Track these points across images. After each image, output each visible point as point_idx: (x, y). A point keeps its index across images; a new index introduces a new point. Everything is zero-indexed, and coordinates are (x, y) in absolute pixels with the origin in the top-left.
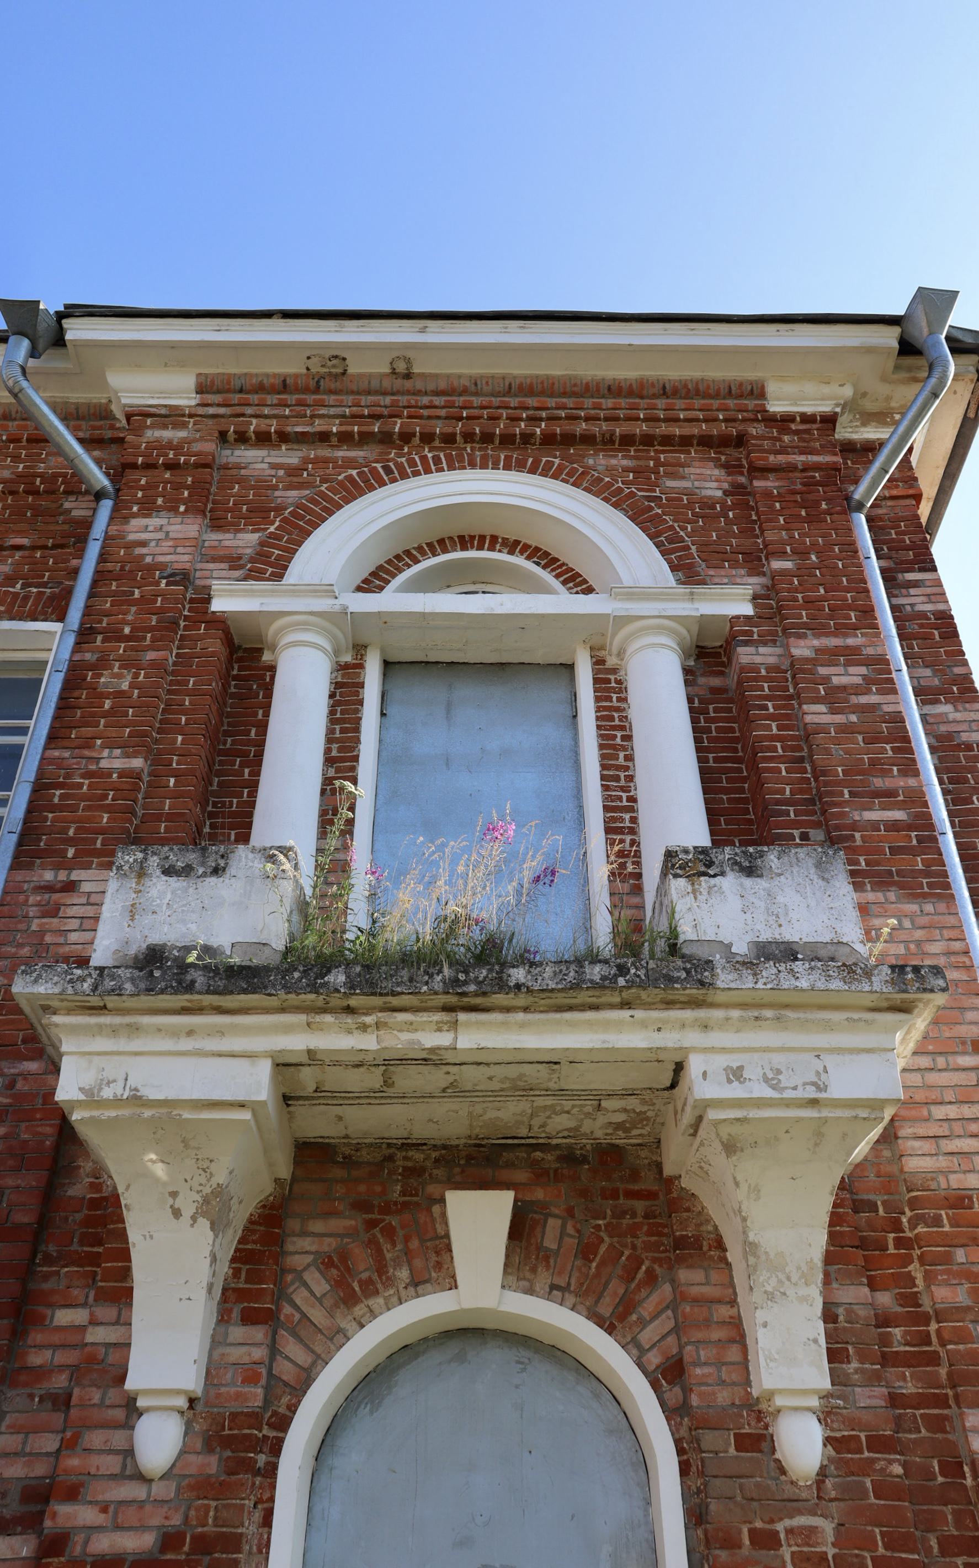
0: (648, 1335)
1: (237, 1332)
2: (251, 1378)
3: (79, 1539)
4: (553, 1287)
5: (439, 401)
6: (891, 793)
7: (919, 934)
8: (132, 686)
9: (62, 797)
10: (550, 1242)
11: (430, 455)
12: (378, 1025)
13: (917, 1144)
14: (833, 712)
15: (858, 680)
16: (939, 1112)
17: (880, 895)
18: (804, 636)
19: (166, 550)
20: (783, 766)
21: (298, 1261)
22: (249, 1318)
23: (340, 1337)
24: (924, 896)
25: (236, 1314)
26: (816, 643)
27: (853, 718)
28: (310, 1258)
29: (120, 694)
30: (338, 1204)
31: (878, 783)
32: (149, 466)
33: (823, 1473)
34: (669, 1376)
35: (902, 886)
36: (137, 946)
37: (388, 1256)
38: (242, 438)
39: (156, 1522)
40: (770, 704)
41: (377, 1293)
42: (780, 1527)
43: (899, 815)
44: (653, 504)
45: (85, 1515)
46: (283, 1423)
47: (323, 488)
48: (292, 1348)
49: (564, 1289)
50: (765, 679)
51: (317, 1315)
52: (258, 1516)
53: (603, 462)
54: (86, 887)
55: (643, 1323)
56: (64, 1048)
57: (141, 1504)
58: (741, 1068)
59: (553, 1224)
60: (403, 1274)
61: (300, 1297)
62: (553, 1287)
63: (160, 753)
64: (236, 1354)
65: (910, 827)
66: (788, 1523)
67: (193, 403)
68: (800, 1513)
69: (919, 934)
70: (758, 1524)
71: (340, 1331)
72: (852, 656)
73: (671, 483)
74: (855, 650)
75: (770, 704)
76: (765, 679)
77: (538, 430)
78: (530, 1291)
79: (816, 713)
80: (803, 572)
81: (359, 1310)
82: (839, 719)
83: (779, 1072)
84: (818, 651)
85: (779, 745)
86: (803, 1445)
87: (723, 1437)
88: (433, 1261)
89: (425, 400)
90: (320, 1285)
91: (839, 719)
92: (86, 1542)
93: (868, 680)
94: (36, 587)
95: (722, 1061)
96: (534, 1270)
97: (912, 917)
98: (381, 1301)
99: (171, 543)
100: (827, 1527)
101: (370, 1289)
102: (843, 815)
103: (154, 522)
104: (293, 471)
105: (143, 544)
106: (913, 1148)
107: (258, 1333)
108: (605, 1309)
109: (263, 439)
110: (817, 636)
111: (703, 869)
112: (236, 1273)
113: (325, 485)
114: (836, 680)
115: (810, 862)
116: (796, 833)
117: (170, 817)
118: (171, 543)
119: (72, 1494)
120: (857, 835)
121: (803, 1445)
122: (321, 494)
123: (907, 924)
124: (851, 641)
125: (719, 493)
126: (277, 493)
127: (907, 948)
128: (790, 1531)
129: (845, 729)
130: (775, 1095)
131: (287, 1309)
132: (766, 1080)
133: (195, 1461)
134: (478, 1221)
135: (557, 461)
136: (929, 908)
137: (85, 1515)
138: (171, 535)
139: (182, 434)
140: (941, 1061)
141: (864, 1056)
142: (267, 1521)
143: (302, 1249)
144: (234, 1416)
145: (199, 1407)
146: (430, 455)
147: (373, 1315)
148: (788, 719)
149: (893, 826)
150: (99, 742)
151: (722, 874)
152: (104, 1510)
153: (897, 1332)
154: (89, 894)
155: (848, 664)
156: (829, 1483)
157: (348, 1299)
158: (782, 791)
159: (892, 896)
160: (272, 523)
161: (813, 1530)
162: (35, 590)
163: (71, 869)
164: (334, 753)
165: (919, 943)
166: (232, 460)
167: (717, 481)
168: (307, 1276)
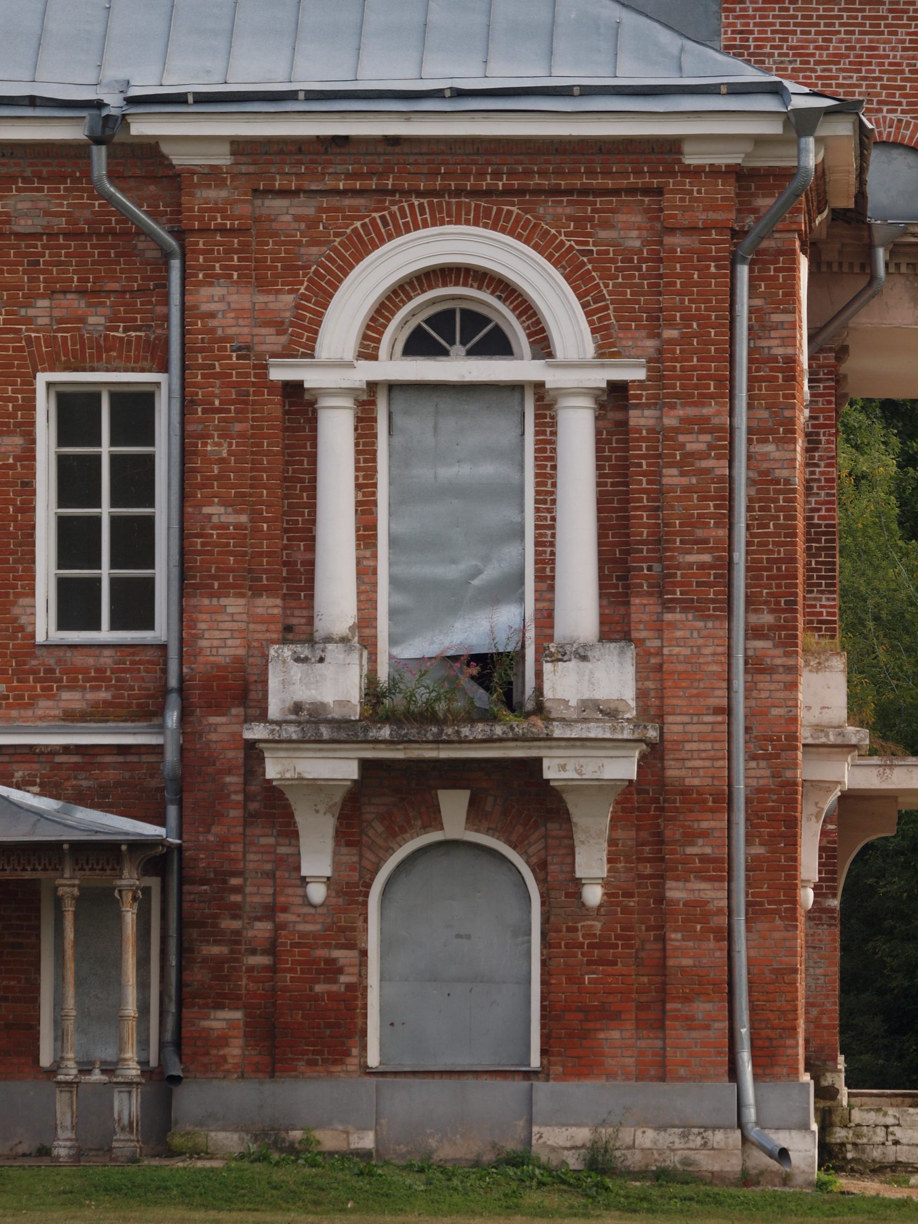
0: (532, 850)
1: (344, 850)
2: (353, 869)
3: (291, 925)
4: (489, 829)
5: (421, 159)
6: (706, 541)
7: (700, 642)
8: (230, 453)
9: (203, 544)
10: (488, 808)
11: (416, 203)
12: (405, 749)
13: (673, 763)
14: (683, 474)
15: (703, 447)
16: (688, 746)
17: (684, 615)
18: (673, 406)
19: (231, 322)
20: (645, 514)
21: (368, 817)
22: (349, 844)
23: (390, 851)
24: (709, 616)
25: (343, 842)
26: (681, 412)
27: (694, 481)
28: (374, 816)
29: (222, 461)
30: (387, 798)
31: (700, 533)
32: (204, 231)
33: (601, 906)
34: (540, 868)
35: (697, 609)
36: (289, 704)
37: (411, 815)
38: (270, 192)
39: (320, 921)
40: (644, 462)
41: (406, 832)
42: (579, 925)
43: (706, 558)
44: (585, 259)
45: (291, 917)
46: (369, 886)
47: (336, 244)
48: (369, 855)
49: (495, 830)
50: (645, 439)
51: (380, 841)
52: (362, 918)
53: (551, 210)
54: (230, 610)
55: (530, 845)
56: (266, 755)
57: (314, 915)
58: (565, 765)
59: (490, 799)
60: (419, 823)
61: (371, 833)
62: (489, 829)
63: (254, 503)
64: (345, 859)
65: (712, 567)
66: (583, 923)
67: (229, 163)
68: (588, 920)
69: (700, 642)
70: (570, 924)
71: (391, 848)
72: (703, 425)
73: (603, 234)
74: (706, 420)
75: (644, 462)
76: (645, 439)
77: (500, 184)
78: (477, 831)
79: (672, 477)
80: (685, 339)
81: (399, 839)
82: (684, 481)
83: (582, 766)
84: (682, 420)
85: (645, 496)
86: (594, 895)
87: (562, 890)
88: (434, 820)
89: (412, 159)
90: (380, 828)
91: (684, 481)
92: (294, 926)
93: (711, 447)
94: (134, 331)
95: (557, 761)
96: (480, 821)
97: (699, 630)
98: (408, 835)
99: (232, 315)
100: (598, 925)
101: (403, 830)
102: (672, 558)
103: (217, 291)
104: (312, 223)
105: (212, 315)
106: (671, 765)
107: (354, 850)
108: (513, 838)
109: (284, 193)
110: (684, 405)
111: (560, 657)
112: (341, 824)
113: (338, 240)
114: (690, 447)
115: (616, 652)
116: (645, 565)
117: (269, 554)
118: (232, 315)
119: (285, 909)
120: (679, 573)
121: (594, 895)
122: (335, 250)
123: (695, 634)
124: (706, 411)
125: (638, 244)
126: (303, 250)
127: (692, 650)
128: (582, 926)
129: (687, 489)
130: (579, 777)
131: (365, 839)
132: (576, 770)
133: (333, 901)
134: (454, 805)
135: (515, 210)
136: (710, 624)
137: (291, 917)
138: (233, 306)
139: (224, 194)
140: (695, 719)
141: (621, 759)
142: (366, 920)
143: (370, 811)
144: (347, 884)
145: (332, 880)
146: (416, 203)
147: (406, 841)
148: (655, 476)
149: (702, 566)
150: (216, 500)
151: (570, 660)
152: (299, 916)
153: (647, 849)
154: (232, 614)
155: (702, 431)
156: (602, 910)
157: (394, 835)
158: (641, 534)
159: (690, 616)
160: (302, 283)
161: (592, 926)
162: (134, 334)
163: (219, 597)
164: (361, 481)
165: (699, 647)
166: (264, 211)
167: (639, 229)
168: (373, 824)
